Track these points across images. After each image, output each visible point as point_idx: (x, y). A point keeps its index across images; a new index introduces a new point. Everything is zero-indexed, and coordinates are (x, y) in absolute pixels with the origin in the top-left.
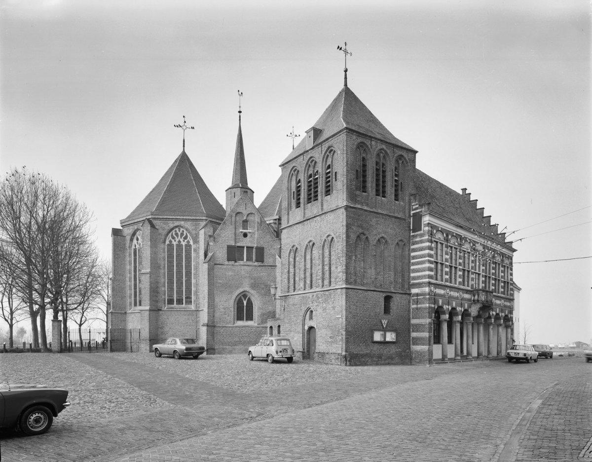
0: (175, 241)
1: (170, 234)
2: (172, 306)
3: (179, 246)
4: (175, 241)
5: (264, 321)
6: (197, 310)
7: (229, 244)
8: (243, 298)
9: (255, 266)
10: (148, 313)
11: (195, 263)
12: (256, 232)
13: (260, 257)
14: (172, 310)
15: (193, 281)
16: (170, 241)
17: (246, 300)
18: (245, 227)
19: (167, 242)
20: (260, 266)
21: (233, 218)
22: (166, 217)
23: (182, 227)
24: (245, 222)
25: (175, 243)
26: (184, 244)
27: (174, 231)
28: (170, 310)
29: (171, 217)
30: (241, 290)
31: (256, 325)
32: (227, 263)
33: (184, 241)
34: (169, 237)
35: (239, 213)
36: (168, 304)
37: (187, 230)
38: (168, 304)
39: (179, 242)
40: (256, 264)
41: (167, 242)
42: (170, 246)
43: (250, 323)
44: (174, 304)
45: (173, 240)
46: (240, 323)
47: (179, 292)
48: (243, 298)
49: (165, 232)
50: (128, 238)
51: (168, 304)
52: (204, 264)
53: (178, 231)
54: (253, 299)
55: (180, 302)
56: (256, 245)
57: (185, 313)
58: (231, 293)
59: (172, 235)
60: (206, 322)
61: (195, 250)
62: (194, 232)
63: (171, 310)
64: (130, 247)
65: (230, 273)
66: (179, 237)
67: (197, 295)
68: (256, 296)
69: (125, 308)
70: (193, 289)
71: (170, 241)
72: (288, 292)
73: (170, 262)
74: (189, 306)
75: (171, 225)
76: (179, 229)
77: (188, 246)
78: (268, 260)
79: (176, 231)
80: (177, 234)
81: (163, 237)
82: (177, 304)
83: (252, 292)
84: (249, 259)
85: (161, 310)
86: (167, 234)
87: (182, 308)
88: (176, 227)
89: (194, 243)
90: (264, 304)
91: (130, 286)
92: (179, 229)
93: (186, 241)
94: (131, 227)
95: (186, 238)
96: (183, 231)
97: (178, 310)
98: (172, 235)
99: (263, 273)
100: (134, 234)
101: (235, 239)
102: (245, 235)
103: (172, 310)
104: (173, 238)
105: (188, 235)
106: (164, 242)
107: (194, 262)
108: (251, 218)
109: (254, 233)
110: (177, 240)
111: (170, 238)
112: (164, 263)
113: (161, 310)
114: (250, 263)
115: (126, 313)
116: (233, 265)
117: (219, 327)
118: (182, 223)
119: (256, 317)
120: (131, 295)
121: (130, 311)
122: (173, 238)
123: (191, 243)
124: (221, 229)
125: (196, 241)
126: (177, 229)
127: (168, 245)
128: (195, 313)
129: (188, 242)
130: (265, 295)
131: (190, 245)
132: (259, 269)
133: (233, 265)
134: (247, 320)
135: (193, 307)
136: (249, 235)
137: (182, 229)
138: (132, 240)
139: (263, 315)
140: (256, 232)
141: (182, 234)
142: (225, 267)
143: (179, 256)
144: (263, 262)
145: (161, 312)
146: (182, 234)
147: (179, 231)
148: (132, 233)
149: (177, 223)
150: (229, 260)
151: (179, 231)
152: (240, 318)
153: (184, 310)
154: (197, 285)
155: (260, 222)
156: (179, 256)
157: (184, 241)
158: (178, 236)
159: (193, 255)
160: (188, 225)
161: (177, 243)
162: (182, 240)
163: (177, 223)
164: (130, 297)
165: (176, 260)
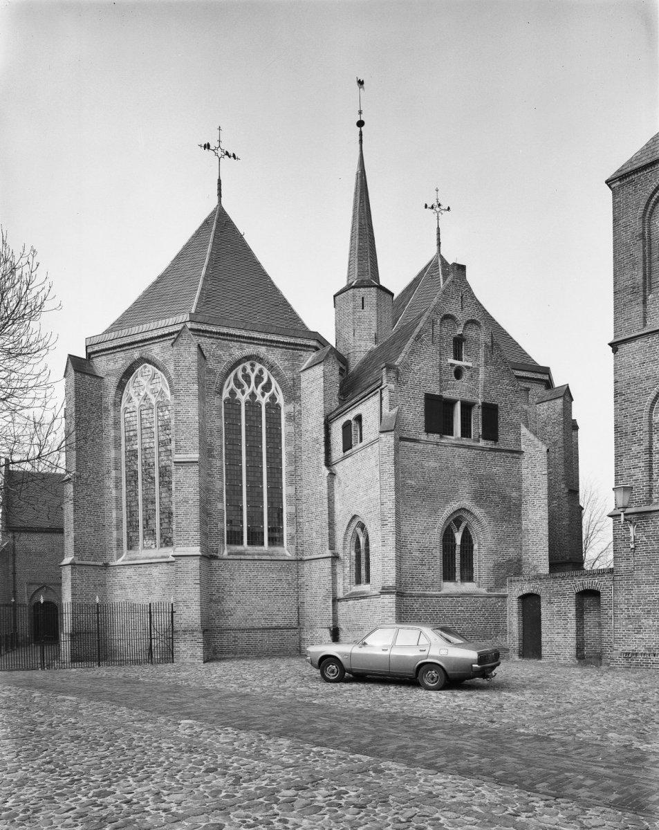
0: (243, 392)
1: (232, 375)
2: (239, 548)
3: (253, 405)
4: (243, 392)
5: (500, 583)
6: (299, 557)
7: (428, 391)
8: (454, 527)
9: (482, 449)
10: (196, 563)
11: (291, 449)
12: (482, 369)
13: (491, 431)
14: (242, 557)
15: (286, 490)
16: (232, 393)
17: (461, 529)
18: (458, 356)
19: (226, 394)
20: (491, 450)
21: (437, 328)
22: (225, 330)
23: (261, 360)
24: (458, 342)
25: (243, 398)
26: (263, 401)
27: (241, 367)
28: (238, 557)
29: (238, 332)
30: (455, 506)
31: (483, 591)
32: (424, 437)
33: (263, 395)
34: (230, 384)
35: (447, 317)
36: (228, 543)
37: (271, 368)
38: (229, 542)
39: (253, 395)
40: (482, 443)
41: (226, 394)
42: (232, 403)
43: (469, 587)
44: (242, 543)
45: (238, 391)
46: (450, 587)
47: (255, 517)
48: (454, 527)
49: (221, 368)
50: (111, 382)
51: (229, 542)
52: (382, 435)
53: (249, 370)
54: (475, 530)
55: (255, 539)
56: (480, 402)
57: (273, 565)
58: (435, 511)
59: (236, 378)
60: (391, 582)
61: (291, 418)
62: (288, 375)
63: (240, 557)
64: (117, 404)
65: (433, 464)
66: (253, 384)
67: (298, 524)
68: (484, 522)
69: (104, 554)
70: (286, 509)
71: (232, 393)
72: (650, 502)
73: (233, 443)
74: (277, 549)
75: (237, 351)
76: (252, 365)
77: (273, 407)
78: (506, 438)
79: (244, 369)
80: (247, 377)
81: (218, 380)
82: (249, 544)
83: (477, 511)
84: (466, 432)
85: (215, 558)
86: (227, 375)
87: (264, 554)
88: (248, 358)
89: (287, 402)
90: (500, 541)
91: (118, 500)
92: (252, 365)
93: (267, 395)
94: (118, 355)
95: (267, 387)
96: (261, 371)
97: (256, 557)
98: (236, 378)
99: (496, 467)
100: (129, 372)
101: (441, 381)
102: (458, 373)
103: (242, 557)
104: (239, 385)
105: (273, 380)
106: (220, 393)
107: (288, 444)
108: (471, 333)
109: (476, 371)
110: (248, 391)
111: (232, 384)
112: (220, 443)
113: (215, 558)
114: (466, 441)
115: (106, 566)
116: (437, 444)
117: (411, 596)
118: (262, 350)
119: (484, 574)
120: (121, 521)
121: (119, 562)
122: (239, 385)
123: (280, 399)
124: (412, 352)
125: (293, 394)
126: (248, 365)
127: (227, 400)
128: (294, 565)
129: (273, 398)
130: (503, 520)
131: (278, 405)
132: (490, 456)
133: (437, 444)
134: (463, 580)
135: (286, 550)
136: (466, 374)
137: (258, 366)
138: (121, 386)
139: (498, 566)
140: (482, 369)
141: (259, 379)
142: (419, 446)
143: (253, 429)
144: (495, 439)
145: (215, 563)
146: (259, 379)
147: (253, 370)
148: (123, 370)
149: (250, 350)
150: (429, 429)
151: (253, 370)
152: (448, 575)
153: (268, 557)
154: (296, 499)
155: (490, 344)
156: (253, 429)
157: (263, 395)
158: (249, 383)
159: (285, 428)
160: (275, 356)
161: (248, 398)
162: (259, 391)
163: (250, 350)
164: (119, 527)
165: (247, 440)
